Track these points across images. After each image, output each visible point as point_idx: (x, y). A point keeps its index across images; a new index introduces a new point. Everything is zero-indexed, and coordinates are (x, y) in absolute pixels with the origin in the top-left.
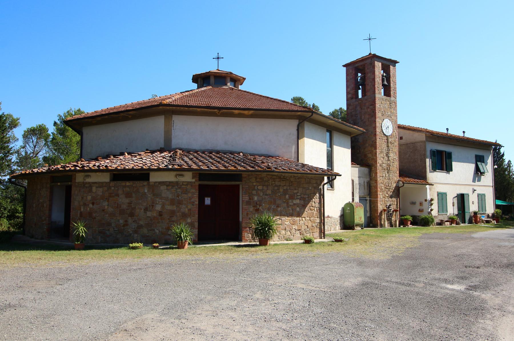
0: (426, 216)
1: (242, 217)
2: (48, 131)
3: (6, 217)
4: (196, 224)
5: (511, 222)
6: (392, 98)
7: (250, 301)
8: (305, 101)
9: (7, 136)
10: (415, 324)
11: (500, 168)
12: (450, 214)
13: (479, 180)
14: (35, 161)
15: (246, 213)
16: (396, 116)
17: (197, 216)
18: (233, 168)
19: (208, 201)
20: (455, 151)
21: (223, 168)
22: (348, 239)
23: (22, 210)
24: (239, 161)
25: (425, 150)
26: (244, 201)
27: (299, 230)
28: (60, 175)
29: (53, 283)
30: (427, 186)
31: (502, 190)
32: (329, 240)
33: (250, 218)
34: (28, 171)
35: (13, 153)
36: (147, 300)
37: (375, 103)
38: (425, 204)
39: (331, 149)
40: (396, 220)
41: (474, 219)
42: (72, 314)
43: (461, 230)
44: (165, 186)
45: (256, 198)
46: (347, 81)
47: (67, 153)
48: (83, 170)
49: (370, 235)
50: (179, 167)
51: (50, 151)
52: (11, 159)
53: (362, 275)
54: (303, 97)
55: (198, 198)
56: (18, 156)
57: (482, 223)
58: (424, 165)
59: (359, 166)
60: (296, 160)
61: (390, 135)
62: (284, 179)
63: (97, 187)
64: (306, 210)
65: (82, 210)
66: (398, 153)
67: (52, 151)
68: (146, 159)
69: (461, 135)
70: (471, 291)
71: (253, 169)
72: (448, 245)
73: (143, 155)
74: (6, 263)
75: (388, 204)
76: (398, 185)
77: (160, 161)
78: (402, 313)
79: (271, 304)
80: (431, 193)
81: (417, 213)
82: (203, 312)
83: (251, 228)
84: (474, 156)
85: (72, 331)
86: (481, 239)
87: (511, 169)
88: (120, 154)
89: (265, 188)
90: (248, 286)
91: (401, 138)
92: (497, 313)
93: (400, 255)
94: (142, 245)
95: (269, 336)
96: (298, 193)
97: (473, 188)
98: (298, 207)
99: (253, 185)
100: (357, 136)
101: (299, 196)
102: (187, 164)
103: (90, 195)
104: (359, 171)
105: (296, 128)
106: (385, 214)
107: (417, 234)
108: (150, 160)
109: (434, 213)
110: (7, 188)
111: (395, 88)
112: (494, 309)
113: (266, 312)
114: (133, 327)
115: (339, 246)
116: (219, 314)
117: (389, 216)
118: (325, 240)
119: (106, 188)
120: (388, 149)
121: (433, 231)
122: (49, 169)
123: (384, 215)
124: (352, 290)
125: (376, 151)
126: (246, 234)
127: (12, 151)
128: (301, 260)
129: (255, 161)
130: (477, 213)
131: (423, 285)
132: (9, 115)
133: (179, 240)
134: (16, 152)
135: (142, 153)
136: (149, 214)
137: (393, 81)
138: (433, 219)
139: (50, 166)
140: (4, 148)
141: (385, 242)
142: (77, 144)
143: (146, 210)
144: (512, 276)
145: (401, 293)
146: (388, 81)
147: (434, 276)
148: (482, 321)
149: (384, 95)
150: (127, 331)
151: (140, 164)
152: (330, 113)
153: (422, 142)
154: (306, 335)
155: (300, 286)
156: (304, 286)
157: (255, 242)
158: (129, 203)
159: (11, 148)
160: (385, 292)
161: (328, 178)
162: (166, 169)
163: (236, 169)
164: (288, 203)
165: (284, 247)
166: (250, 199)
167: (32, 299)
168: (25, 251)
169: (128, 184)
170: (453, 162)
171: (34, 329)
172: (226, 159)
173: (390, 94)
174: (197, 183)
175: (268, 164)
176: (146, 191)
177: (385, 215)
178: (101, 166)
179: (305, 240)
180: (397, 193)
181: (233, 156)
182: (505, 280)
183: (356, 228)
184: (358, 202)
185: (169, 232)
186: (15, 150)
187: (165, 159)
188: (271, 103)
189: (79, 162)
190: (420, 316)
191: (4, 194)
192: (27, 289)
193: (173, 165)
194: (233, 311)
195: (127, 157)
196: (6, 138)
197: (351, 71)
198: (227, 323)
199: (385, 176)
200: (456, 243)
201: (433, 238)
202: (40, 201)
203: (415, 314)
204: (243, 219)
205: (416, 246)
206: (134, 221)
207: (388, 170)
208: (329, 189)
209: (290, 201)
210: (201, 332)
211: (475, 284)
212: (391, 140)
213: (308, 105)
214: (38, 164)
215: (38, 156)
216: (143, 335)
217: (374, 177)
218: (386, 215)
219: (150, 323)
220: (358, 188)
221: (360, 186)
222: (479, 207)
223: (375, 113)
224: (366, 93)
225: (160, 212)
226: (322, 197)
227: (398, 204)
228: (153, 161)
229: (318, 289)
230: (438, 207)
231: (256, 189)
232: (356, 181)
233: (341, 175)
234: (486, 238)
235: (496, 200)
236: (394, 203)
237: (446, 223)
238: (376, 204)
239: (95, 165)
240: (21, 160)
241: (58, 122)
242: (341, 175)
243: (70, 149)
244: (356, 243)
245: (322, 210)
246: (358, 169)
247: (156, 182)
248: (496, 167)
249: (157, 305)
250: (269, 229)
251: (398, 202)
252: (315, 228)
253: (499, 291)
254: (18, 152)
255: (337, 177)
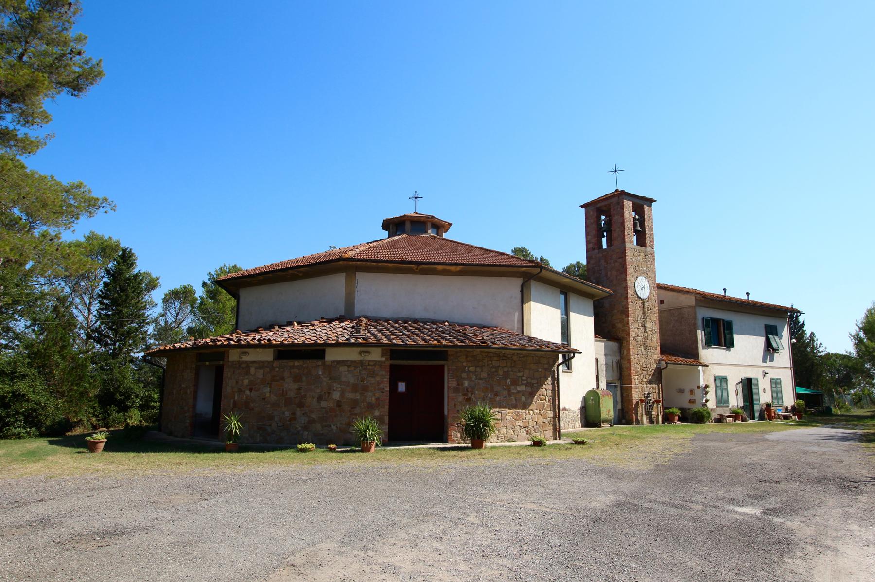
0: (699, 409)
1: (448, 409)
2: (194, 294)
3: (138, 407)
4: (387, 419)
5: (819, 418)
6: (648, 249)
7: (461, 526)
8: (530, 253)
9: (143, 300)
10: (694, 563)
11: (799, 343)
12: (733, 406)
13: (772, 360)
14: (177, 332)
15: (453, 404)
16: (654, 272)
17: (387, 407)
18: (435, 343)
19: (402, 387)
20: (736, 320)
21: (422, 343)
22: (592, 441)
23: (158, 398)
24: (444, 333)
25: (695, 318)
26: (450, 387)
27: (526, 427)
28: (209, 352)
29: (196, 497)
30: (700, 368)
31: (804, 373)
32: (566, 442)
33: (458, 411)
34: (169, 346)
35: (150, 323)
36: (322, 523)
37: (625, 256)
38: (698, 393)
39: (567, 317)
40: (658, 414)
41: (767, 413)
42: (221, 541)
43: (750, 429)
44: (346, 367)
45: (466, 383)
46: (587, 226)
47: (218, 323)
48: (239, 345)
49: (623, 435)
50: (364, 342)
51: (197, 320)
52: (147, 331)
53: (615, 492)
54: (527, 248)
55: (389, 382)
56: (156, 326)
57: (778, 420)
58: (694, 338)
59: (605, 340)
60: (519, 332)
61: (647, 298)
62: (504, 358)
63: (256, 368)
64: (535, 399)
65: (236, 398)
66: (657, 322)
67: (199, 319)
68: (321, 331)
69: (744, 297)
70: (770, 517)
71: (463, 344)
72: (732, 449)
73: (317, 325)
74: (135, 470)
75: (647, 393)
76: (659, 366)
77: (339, 333)
78: (675, 547)
79: (490, 532)
80: (705, 377)
81: (687, 405)
82: (398, 542)
83: (460, 424)
84: (764, 326)
85: (221, 565)
86: (778, 441)
87: (815, 344)
88: (287, 324)
89: (479, 370)
90: (458, 505)
91: (662, 302)
92: (811, 549)
93: (666, 463)
94: (313, 446)
95: (489, 578)
96: (523, 376)
97: (763, 371)
98: (523, 395)
99: (463, 366)
100: (601, 299)
101: (525, 380)
102: (375, 337)
103: (247, 378)
104: (606, 347)
105: (520, 289)
106: (642, 406)
107: (688, 434)
108: (326, 331)
109: (711, 405)
110: (141, 368)
111: (652, 235)
112: (805, 544)
113: (483, 543)
114: (303, 562)
115: (581, 450)
116: (420, 544)
117: (648, 409)
118: (562, 442)
119: (268, 369)
120: (644, 317)
121: (710, 430)
122: (195, 343)
123: (641, 408)
124: (601, 512)
125: (628, 320)
126: (453, 432)
127: (148, 320)
128: (528, 469)
129: (465, 333)
130: (771, 405)
131: (702, 506)
132: (147, 273)
133: (363, 440)
134: (153, 322)
135: (316, 323)
136: (324, 404)
137: (648, 226)
138: (709, 414)
139: (196, 339)
140: (139, 315)
141: (644, 444)
142: (231, 311)
143: (320, 398)
144: (826, 495)
145: (671, 519)
146: (643, 225)
147: (717, 494)
148: (789, 561)
149: (638, 244)
150: (294, 566)
151: (313, 337)
152: (563, 269)
153: (690, 307)
154: (541, 577)
155: (529, 506)
156: (535, 507)
157: (466, 443)
158: (297, 389)
159: (148, 316)
160: (649, 517)
161: (564, 356)
162: (348, 344)
163: (439, 344)
164: (509, 391)
165: (506, 451)
166: (458, 385)
167: (169, 518)
168: (160, 454)
169: (297, 363)
170: (734, 335)
171: (171, 561)
172: (427, 331)
173: (646, 243)
174: (388, 363)
175: (483, 338)
176: (320, 373)
177: (642, 408)
178: (262, 339)
179: (533, 441)
180: (658, 377)
181: (435, 326)
182: (817, 500)
183: (602, 426)
184: (605, 389)
185: (350, 429)
186: (152, 318)
187: (345, 331)
188: (485, 256)
189: (234, 335)
190: (700, 553)
191: (137, 376)
192: (162, 505)
193: (357, 338)
194: (438, 540)
195: (296, 328)
196: (142, 303)
197: (591, 213)
198: (431, 558)
199: (641, 353)
200: (743, 448)
201: (711, 441)
202: (183, 386)
203: (693, 548)
204: (450, 412)
205: (687, 451)
206: (304, 414)
207: (646, 346)
208: (564, 371)
209: (513, 387)
210: (396, 571)
211: (775, 506)
212: (648, 304)
213: (534, 259)
214: (180, 337)
215: (181, 327)
216: (316, 573)
217: (626, 355)
218: (643, 407)
219: (326, 555)
220: (605, 369)
221: (606, 367)
222: (772, 397)
223: (626, 268)
224: (613, 242)
225: (338, 401)
226: (556, 382)
227: (661, 393)
228: (330, 333)
229: (555, 511)
230: (716, 396)
231: (467, 371)
232: (602, 361)
233: (581, 353)
234: (785, 440)
235: (797, 387)
236: (654, 391)
237: (727, 418)
238: (630, 392)
239: (254, 339)
240: (159, 331)
241: (208, 282)
242: (581, 353)
243: (222, 318)
244: (604, 446)
245: (557, 401)
246: (603, 343)
247: (334, 361)
248: (794, 341)
249: (335, 530)
250: (485, 426)
251: (660, 390)
252: (546, 425)
253: (810, 516)
254: (155, 321)
255: (576, 354)
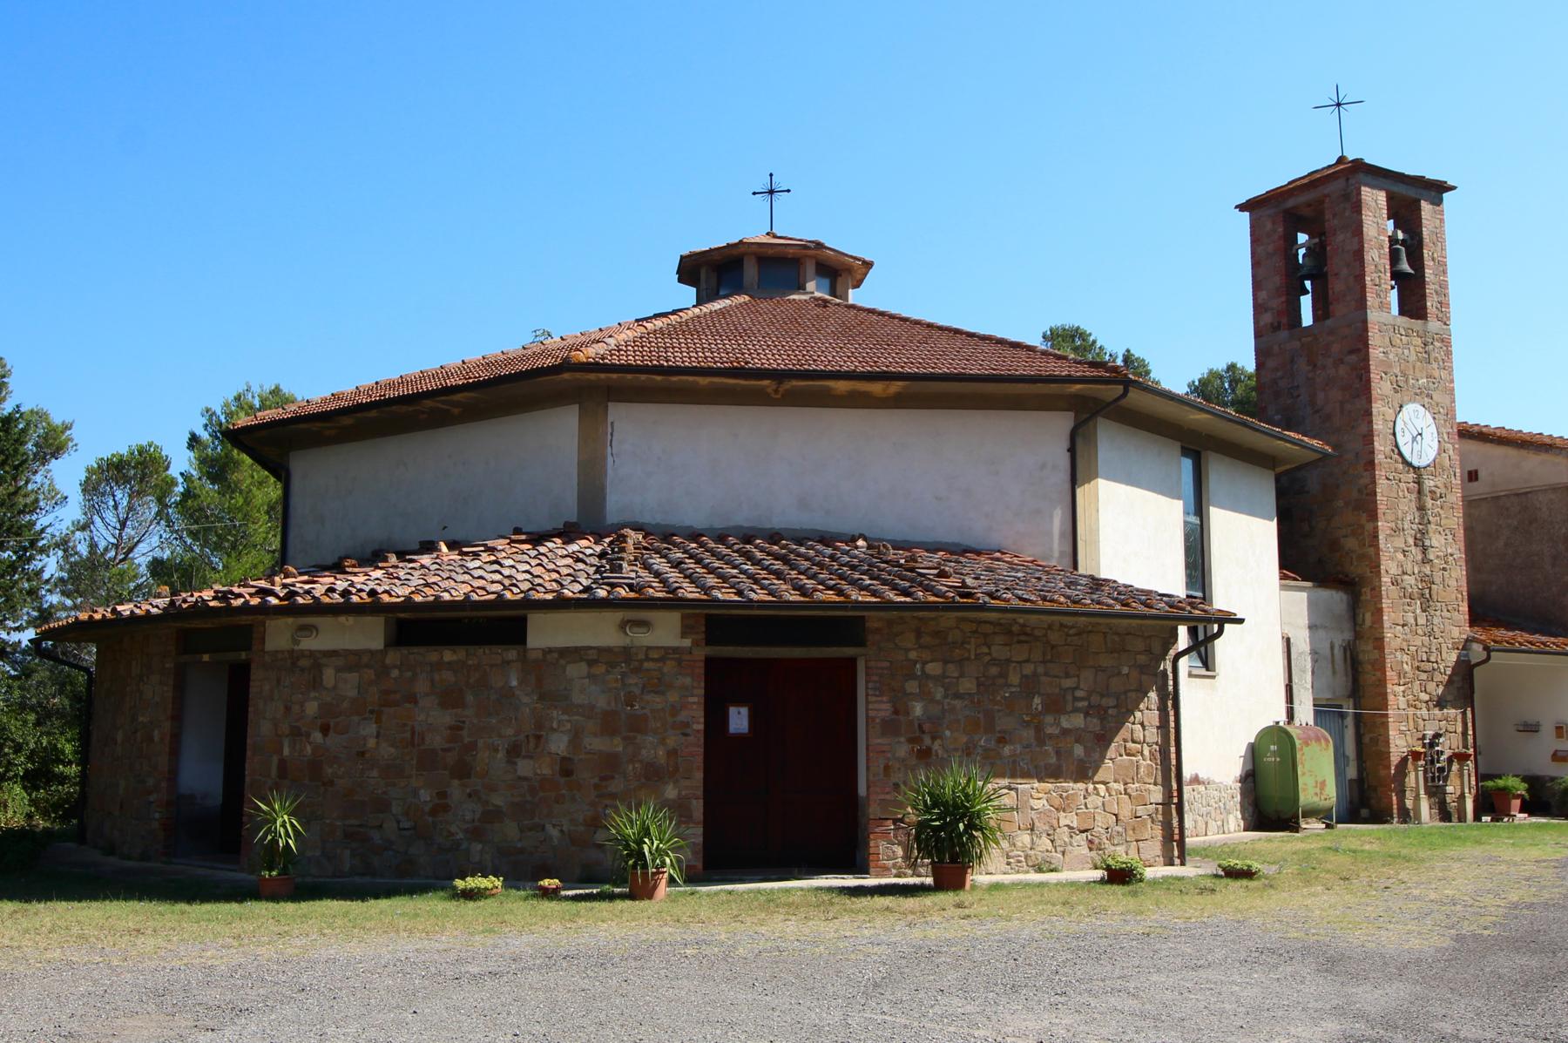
1: (868, 780)
2: (167, 468)
3: (22, 777)
4: (698, 808)
6: (1433, 325)
8: (1094, 342)
9: (30, 487)
14: (122, 574)
15: (882, 766)
17: (699, 775)
18: (831, 596)
19: (739, 720)
21: (794, 597)
22: (1274, 868)
23: (76, 752)
24: (853, 568)
26: (873, 719)
28: (209, 625)
29: (184, 1021)
32: (1201, 871)
33: (896, 786)
34: (101, 610)
35: (49, 547)
37: (1366, 346)
39: (1201, 521)
44: (583, 666)
45: (918, 709)
46: (1256, 263)
47: (234, 547)
48: (290, 608)
49: (1362, 851)
50: (632, 595)
51: (176, 539)
52: (42, 570)
53: (1339, 1012)
54: (1086, 326)
55: (702, 707)
56: (66, 557)
59: (1309, 584)
60: (1066, 563)
61: (1429, 466)
62: (1023, 638)
63: (338, 670)
64: (1111, 752)
65: (286, 751)
66: (1461, 533)
67: (181, 538)
68: (513, 567)
71: (908, 599)
73: (503, 550)
74: (19, 947)
75: (1430, 733)
76: (1467, 655)
77: (565, 571)
83: (902, 820)
88: (421, 548)
89: (952, 670)
91: (1473, 476)
93: (1486, 933)
94: (498, 883)
96: (1077, 688)
98: (1077, 741)
99: (908, 660)
100: (1299, 468)
101: (1082, 699)
102: (664, 582)
103: (315, 699)
104: (1312, 605)
105: (1065, 444)
106: (1416, 771)
108: (527, 567)
110: (27, 673)
111: (1443, 286)
115: (1242, 892)
117: (1433, 779)
118: (1188, 871)
119: (370, 674)
120: (1422, 517)
122: (172, 603)
126: (882, 845)
127: (44, 542)
128: (1095, 947)
129: (912, 570)
132: (37, 413)
133: (634, 866)
134: (57, 545)
135: (500, 544)
136: (524, 767)
137: (1433, 259)
139: (174, 593)
140: (19, 528)
142: (268, 513)
143: (514, 752)
149: (1402, 312)
151: (493, 582)
152: (1189, 386)
157: (919, 876)
158: (451, 728)
159: (43, 531)
161: (1193, 632)
162: (587, 603)
163: (842, 599)
164: (1039, 729)
166: (896, 712)
168: (84, 904)
169: (448, 655)
172: (807, 564)
174: (701, 653)
175: (963, 582)
176: (514, 683)
178: (354, 591)
179: (1108, 868)
181: (829, 551)
183: (1304, 826)
184: (1311, 722)
185: (597, 835)
186: (53, 536)
187: (581, 566)
188: (968, 351)
189: (277, 579)
191: (17, 693)
193: (613, 586)
195: (445, 559)
196: (26, 496)
197: (1269, 226)
199: (1412, 621)
202: (141, 719)
204: (871, 789)
205: (1547, 896)
206: (470, 795)
207: (1427, 602)
208: (1195, 672)
209: (1049, 719)
212: (1432, 483)
213: (1107, 358)
214: (132, 585)
215: (133, 559)
217: (1371, 627)
218: (1421, 774)
221: (1315, 662)
223: (1369, 381)
224: (1331, 307)
225: (564, 759)
227: (1470, 732)
228: (538, 571)
231: (919, 673)
232: (1302, 643)
233: (1241, 621)
236: (1451, 729)
239: (331, 590)
240: (74, 571)
241: (205, 436)
242: (1241, 621)
243: (244, 532)
244: (1308, 883)
245: (1173, 756)
247: (550, 650)
250: (971, 826)
251: (1470, 725)
254: (64, 544)
255: (1227, 626)
